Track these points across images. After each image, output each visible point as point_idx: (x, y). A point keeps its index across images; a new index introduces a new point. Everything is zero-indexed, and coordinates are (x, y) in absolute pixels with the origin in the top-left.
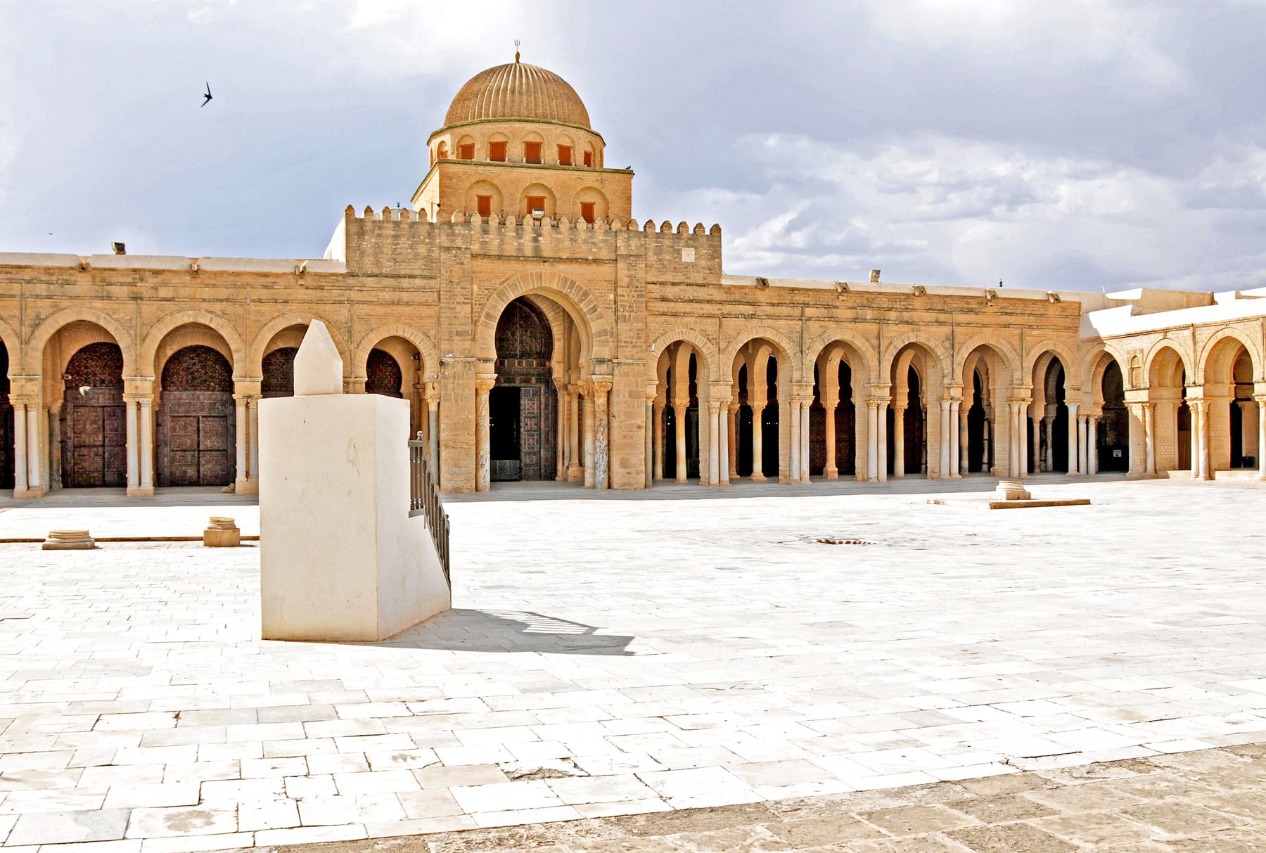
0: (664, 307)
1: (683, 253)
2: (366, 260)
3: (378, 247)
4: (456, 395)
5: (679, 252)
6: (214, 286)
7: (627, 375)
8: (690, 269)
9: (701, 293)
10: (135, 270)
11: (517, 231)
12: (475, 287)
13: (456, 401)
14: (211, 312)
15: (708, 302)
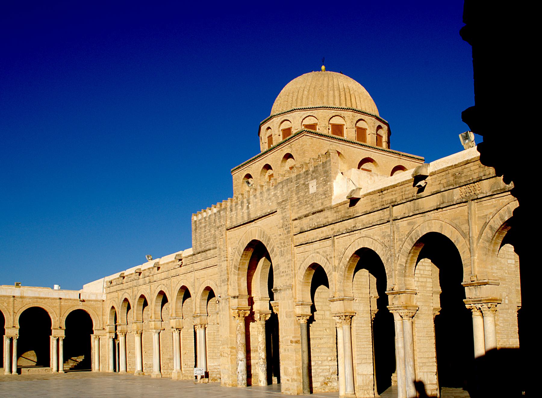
0: (302, 238)
1: (310, 186)
8: (314, 198)
9: (320, 219)
14: (164, 285)
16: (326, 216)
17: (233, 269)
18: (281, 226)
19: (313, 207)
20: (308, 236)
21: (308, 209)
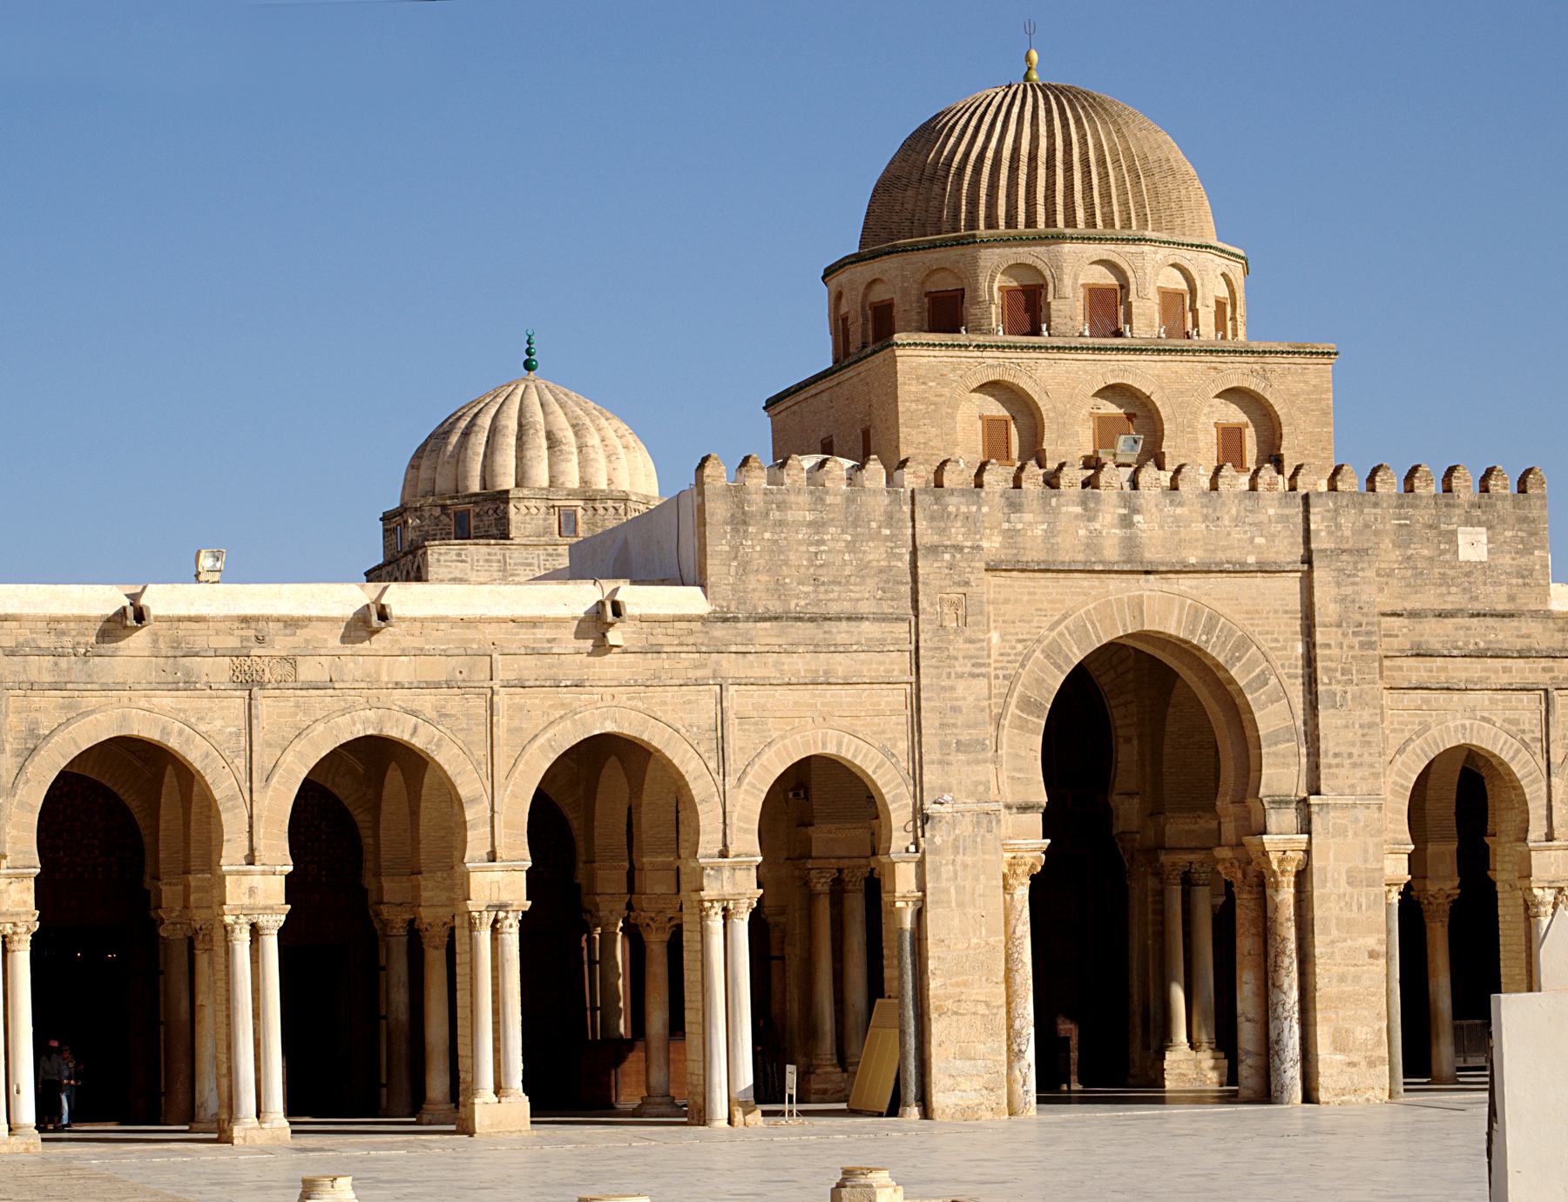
0: (1417, 670)
2: (752, 582)
3: (775, 548)
4: (960, 890)
5: (1451, 537)
6: (420, 653)
7: (1342, 832)
9: (1504, 634)
10: (245, 620)
11: (1084, 504)
12: (995, 637)
13: (961, 905)
14: (414, 713)
15: (1522, 655)
16: (1524, 631)
17: (1013, 709)
18: (1334, 618)
19: (1476, 598)
20: (1440, 669)
21: (1450, 598)
